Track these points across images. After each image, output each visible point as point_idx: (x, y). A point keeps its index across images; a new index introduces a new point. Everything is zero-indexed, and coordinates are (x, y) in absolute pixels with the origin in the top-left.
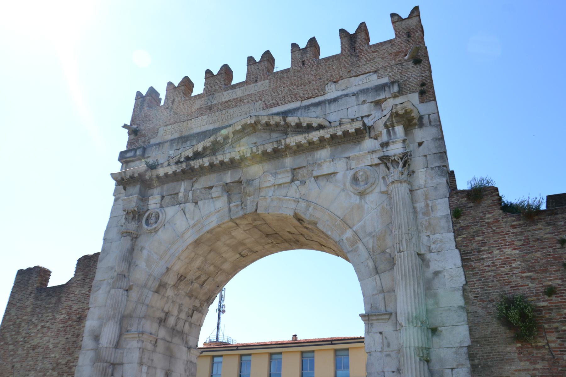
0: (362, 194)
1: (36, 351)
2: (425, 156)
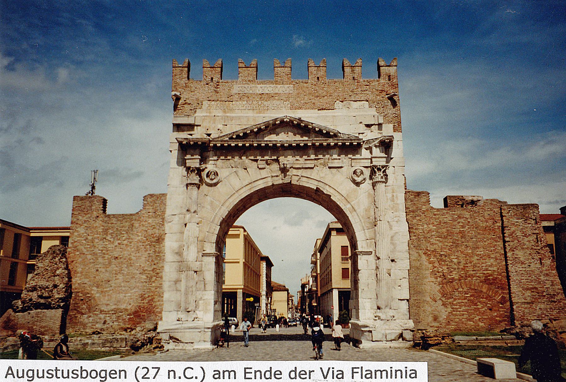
0: (358, 184)
1: (118, 261)
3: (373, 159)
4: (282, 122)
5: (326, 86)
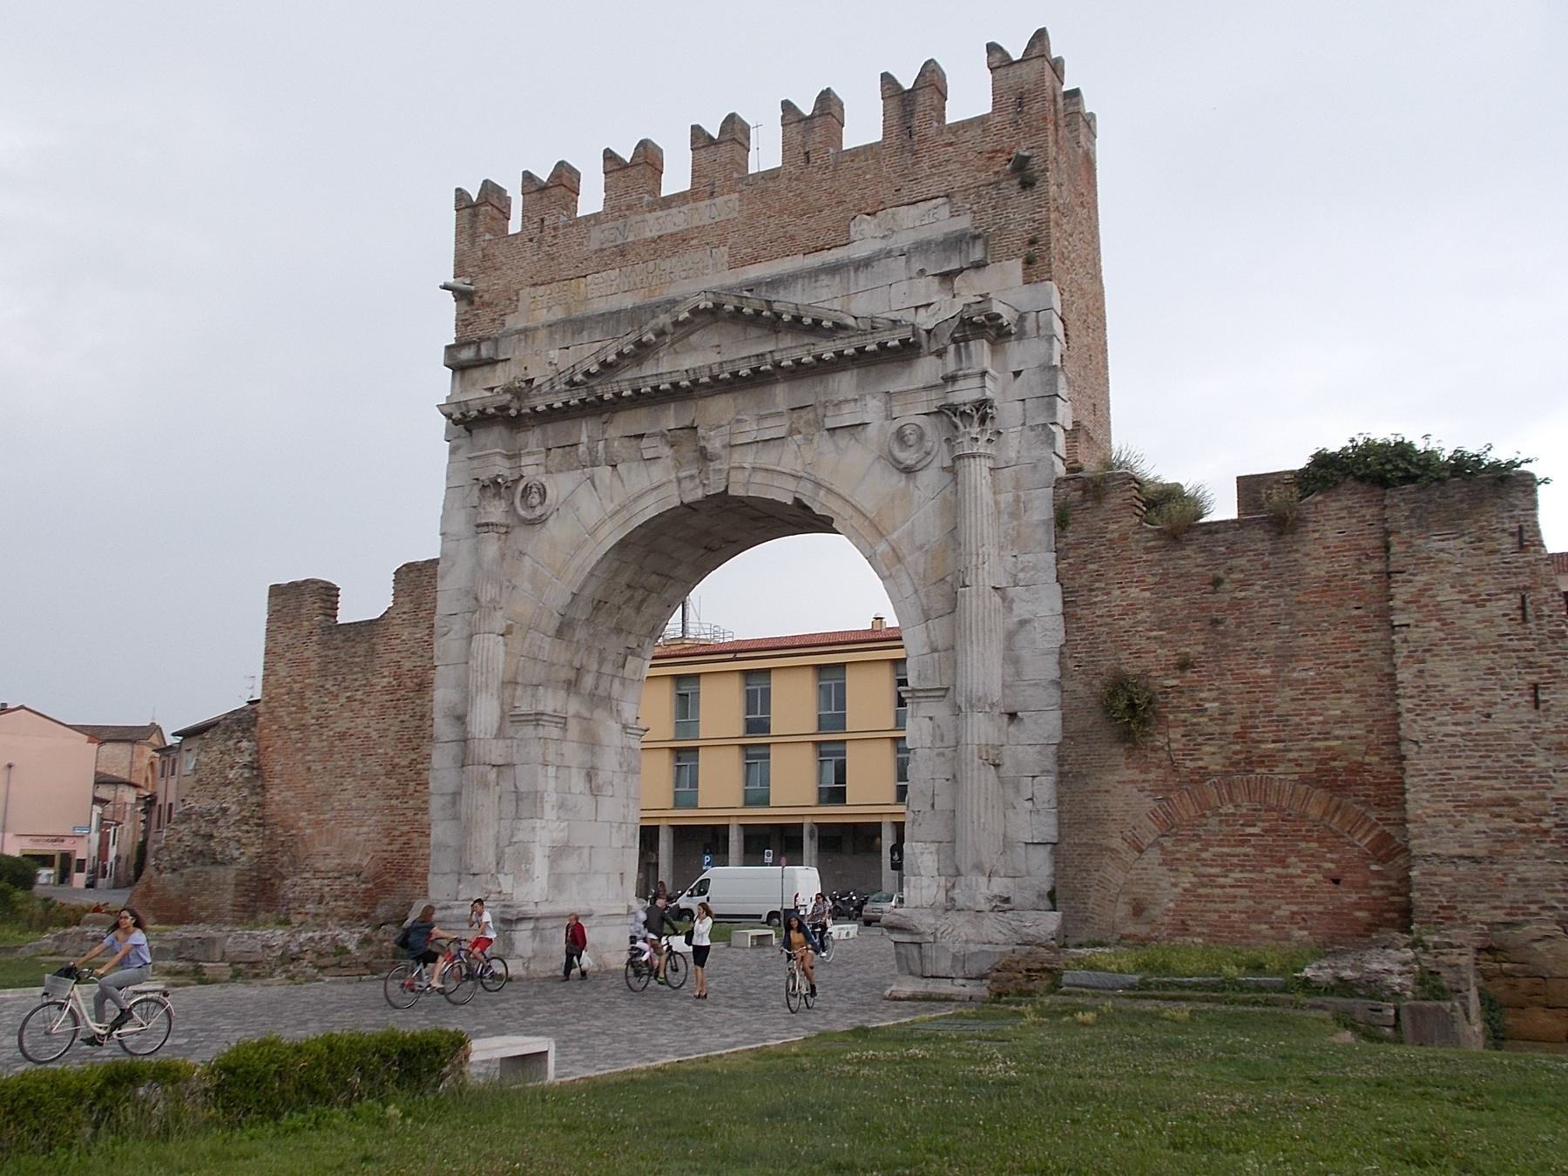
0: (908, 471)
4: (695, 311)
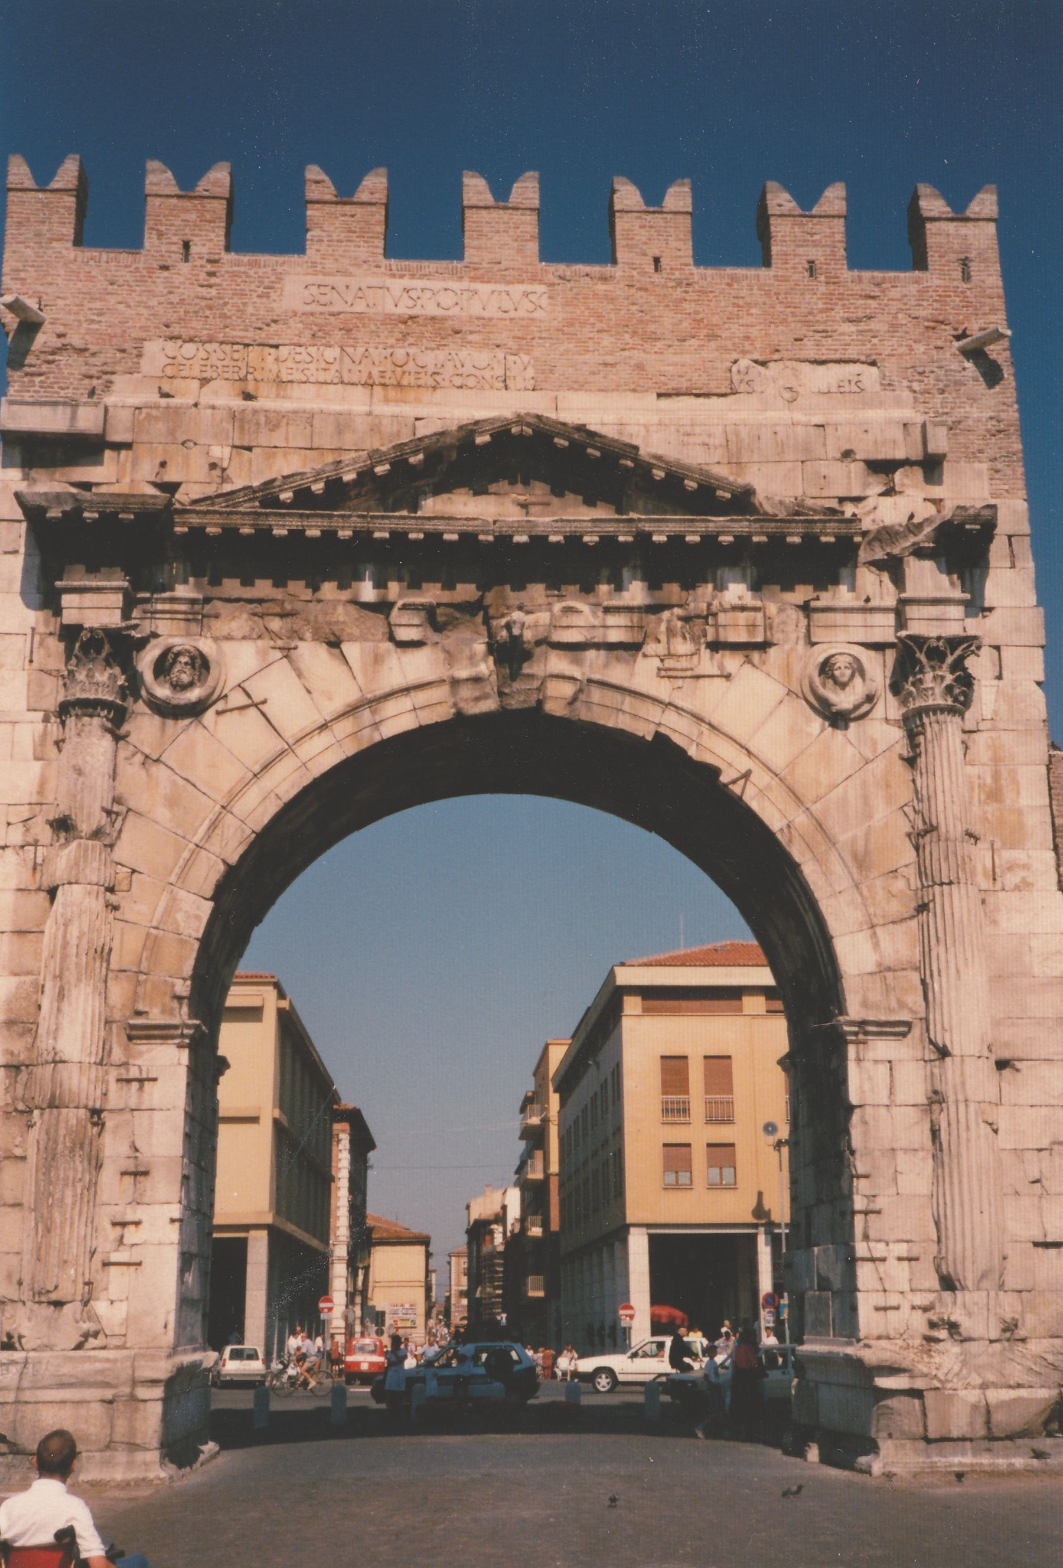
2: (997, 648)
3: (912, 611)
5: (692, 296)
